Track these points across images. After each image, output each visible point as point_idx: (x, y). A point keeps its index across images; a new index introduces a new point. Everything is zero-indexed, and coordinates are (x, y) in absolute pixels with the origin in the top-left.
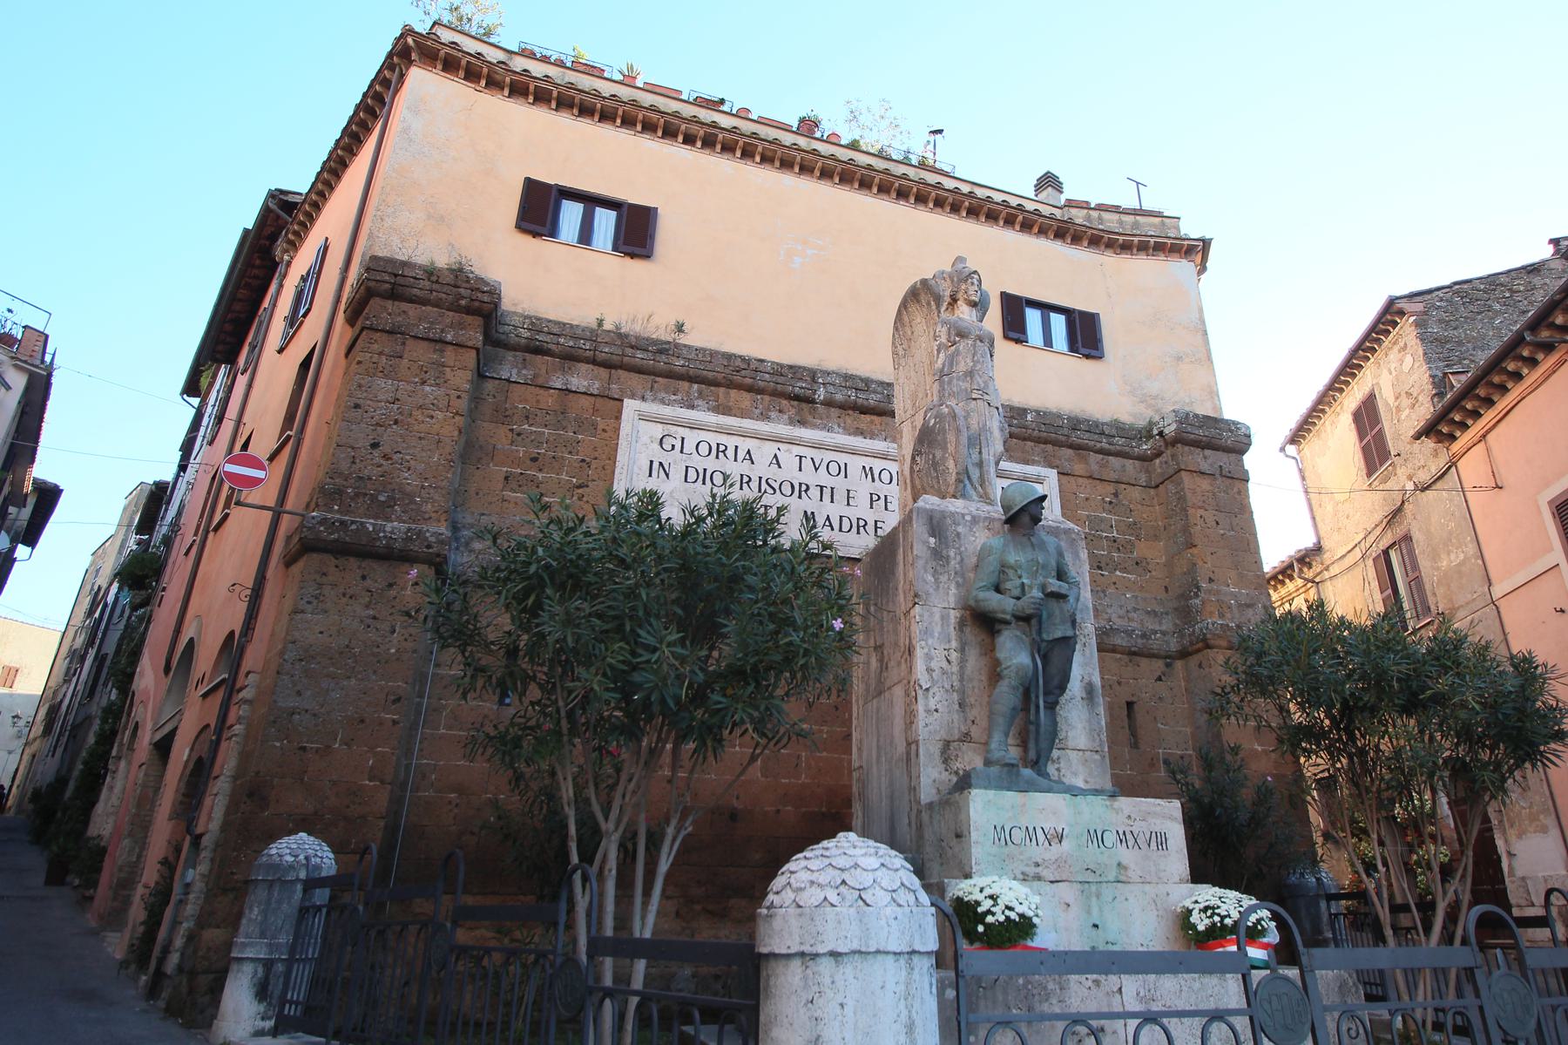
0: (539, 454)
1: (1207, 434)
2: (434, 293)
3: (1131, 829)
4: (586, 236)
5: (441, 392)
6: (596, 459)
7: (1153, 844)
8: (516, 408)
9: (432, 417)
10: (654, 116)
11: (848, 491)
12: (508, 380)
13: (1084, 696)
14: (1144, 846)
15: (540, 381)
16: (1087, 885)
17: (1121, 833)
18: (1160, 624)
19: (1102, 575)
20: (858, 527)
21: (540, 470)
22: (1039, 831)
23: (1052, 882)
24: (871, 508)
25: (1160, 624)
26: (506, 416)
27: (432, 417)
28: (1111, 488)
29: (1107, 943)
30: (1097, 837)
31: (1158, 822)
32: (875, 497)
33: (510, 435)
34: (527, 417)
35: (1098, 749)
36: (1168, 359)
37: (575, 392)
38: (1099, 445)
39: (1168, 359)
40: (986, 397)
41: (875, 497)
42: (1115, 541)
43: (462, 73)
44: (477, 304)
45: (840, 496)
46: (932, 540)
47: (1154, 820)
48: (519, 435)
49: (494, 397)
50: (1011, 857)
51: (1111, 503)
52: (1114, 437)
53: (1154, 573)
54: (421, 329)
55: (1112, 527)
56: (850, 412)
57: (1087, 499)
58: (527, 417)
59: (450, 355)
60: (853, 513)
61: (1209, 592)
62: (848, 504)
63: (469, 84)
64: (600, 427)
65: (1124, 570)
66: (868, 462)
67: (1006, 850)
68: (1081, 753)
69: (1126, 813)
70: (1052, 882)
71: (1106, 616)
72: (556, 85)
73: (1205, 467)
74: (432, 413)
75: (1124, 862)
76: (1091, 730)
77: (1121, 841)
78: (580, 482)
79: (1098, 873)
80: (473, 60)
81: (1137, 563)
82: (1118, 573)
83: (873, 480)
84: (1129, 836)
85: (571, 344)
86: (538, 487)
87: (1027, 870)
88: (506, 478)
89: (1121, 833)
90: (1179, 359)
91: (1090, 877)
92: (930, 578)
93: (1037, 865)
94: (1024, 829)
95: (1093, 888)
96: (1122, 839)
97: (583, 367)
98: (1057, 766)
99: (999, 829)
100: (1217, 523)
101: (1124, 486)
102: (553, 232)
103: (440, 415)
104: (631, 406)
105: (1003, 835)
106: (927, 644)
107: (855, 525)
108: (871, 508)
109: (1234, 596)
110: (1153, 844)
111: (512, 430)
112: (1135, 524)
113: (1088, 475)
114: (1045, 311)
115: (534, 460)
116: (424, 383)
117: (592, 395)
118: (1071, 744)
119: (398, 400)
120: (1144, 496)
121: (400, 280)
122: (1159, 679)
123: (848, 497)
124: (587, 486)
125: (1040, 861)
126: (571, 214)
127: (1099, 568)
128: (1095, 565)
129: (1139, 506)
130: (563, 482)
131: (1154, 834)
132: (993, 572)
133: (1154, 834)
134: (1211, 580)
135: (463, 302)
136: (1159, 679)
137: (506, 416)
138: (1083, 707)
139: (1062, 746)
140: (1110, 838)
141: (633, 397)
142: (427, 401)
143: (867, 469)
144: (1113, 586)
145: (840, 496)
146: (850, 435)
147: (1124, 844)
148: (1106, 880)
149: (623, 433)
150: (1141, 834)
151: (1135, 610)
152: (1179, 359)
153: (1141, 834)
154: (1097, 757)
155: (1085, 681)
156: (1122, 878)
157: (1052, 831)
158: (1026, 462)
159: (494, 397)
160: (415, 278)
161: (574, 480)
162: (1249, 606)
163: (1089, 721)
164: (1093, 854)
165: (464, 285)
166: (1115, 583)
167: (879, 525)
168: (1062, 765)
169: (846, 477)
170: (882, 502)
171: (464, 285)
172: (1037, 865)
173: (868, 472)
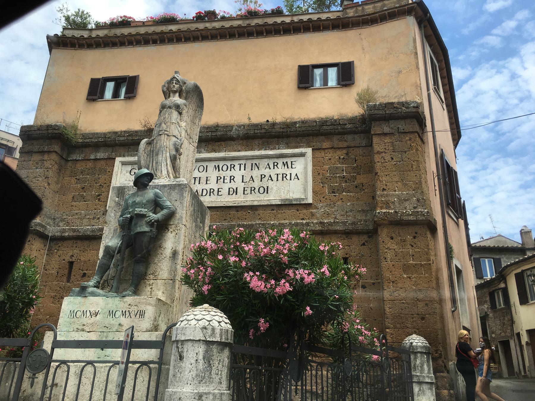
0: (85, 186)
1: (387, 112)
2: (41, 135)
3: (129, 309)
4: (116, 95)
5: (42, 170)
6: (105, 183)
7: (138, 316)
8: (78, 170)
9: (38, 180)
10: (138, 37)
11: (207, 178)
12: (75, 160)
13: (171, 256)
14: (133, 316)
15: (86, 158)
16: (103, 333)
17: (124, 311)
18: (366, 216)
19: (335, 196)
20: (210, 192)
21: (85, 192)
22: (88, 312)
23: (88, 332)
24: (217, 183)
25: (366, 216)
26: (75, 174)
27: (38, 180)
28: (345, 151)
29: (105, 356)
30: (112, 313)
31: (142, 306)
32: (219, 178)
33: (76, 180)
34: (82, 173)
35: (172, 278)
36: (394, 74)
37: (99, 159)
38: (337, 131)
39: (394, 74)
40: (166, 132)
41: (219, 178)
42: (344, 178)
43: (69, 46)
44: (54, 135)
45: (203, 180)
46: (117, 199)
47: (141, 306)
48: (78, 180)
49: (71, 167)
50: (74, 322)
51: (344, 158)
52: (346, 124)
53: (366, 190)
54: (36, 150)
55: (343, 171)
56: (211, 142)
57: (330, 159)
58: (82, 173)
59: (46, 157)
60: (208, 187)
61: (382, 196)
62: (207, 183)
63: (72, 49)
64: (108, 171)
65: (349, 191)
66: (216, 163)
67: (73, 320)
68: (164, 281)
69: (129, 303)
70: (88, 332)
71: (334, 216)
72: (101, 38)
73: (387, 130)
74: (39, 179)
75: (122, 323)
76: (171, 270)
77: (123, 315)
78: (99, 194)
79: (109, 328)
80: (71, 39)
81: (356, 187)
82: (344, 193)
83: (219, 171)
84: (127, 313)
85: (96, 140)
86: (84, 198)
87: (79, 327)
88: (73, 197)
89: (124, 311)
90: (400, 72)
91: (105, 330)
92: (113, 215)
93: (84, 325)
94: (82, 311)
95: (105, 334)
96: (124, 314)
97: (102, 149)
98: (151, 287)
99: (72, 312)
100: (392, 159)
101: (352, 149)
102: (102, 96)
103: (40, 179)
104: (118, 160)
105: (73, 314)
106: (105, 242)
107: (209, 192)
108: (217, 183)
109: (398, 196)
110: (138, 316)
111: (76, 179)
112: (357, 166)
113: (331, 147)
114: (325, 68)
115: (83, 188)
116: (37, 168)
117: (105, 159)
118: (159, 277)
119: (28, 176)
120: (364, 151)
121: (30, 133)
122: (364, 244)
123: (207, 180)
124: (101, 195)
125: (85, 323)
126: (110, 86)
127: (333, 192)
128: (331, 191)
129: (361, 157)
130: (93, 195)
131: (139, 311)
132: (124, 208)
133: (139, 311)
134: (384, 190)
135: (50, 135)
136: (364, 244)
137: (75, 174)
138: (170, 260)
139: (155, 278)
140: (118, 314)
141: (120, 156)
142: (37, 175)
143: (217, 166)
144: (341, 201)
145: (203, 180)
146: (209, 152)
147: (124, 316)
148: (112, 331)
149: (114, 171)
150: (133, 312)
151: (351, 211)
152: (400, 72)
153: (133, 312)
154: (171, 282)
155: (173, 249)
156: (120, 330)
157: (94, 312)
158: (297, 147)
159: (71, 167)
160: (34, 131)
161: (97, 194)
162: (406, 200)
163: (171, 267)
164: (110, 321)
165: (50, 129)
166: (342, 199)
167: (220, 190)
168: (153, 286)
169: (206, 171)
170: (222, 180)
171: (50, 129)
172: (84, 325)
173: (217, 168)
